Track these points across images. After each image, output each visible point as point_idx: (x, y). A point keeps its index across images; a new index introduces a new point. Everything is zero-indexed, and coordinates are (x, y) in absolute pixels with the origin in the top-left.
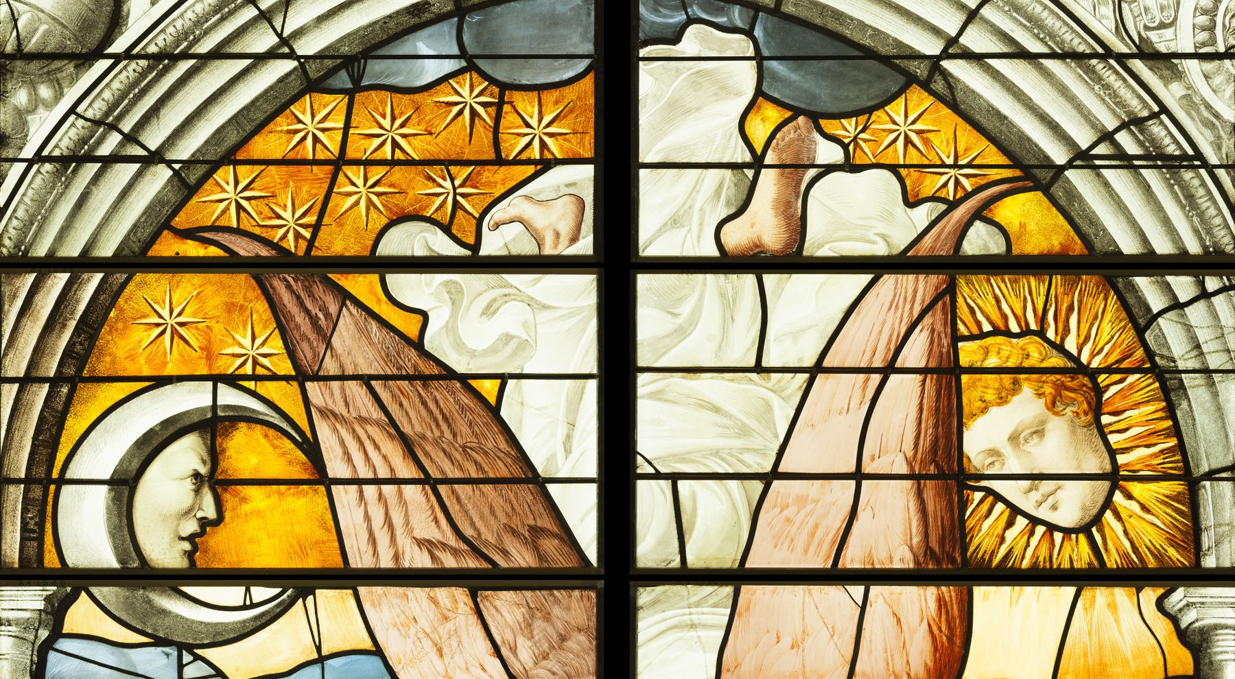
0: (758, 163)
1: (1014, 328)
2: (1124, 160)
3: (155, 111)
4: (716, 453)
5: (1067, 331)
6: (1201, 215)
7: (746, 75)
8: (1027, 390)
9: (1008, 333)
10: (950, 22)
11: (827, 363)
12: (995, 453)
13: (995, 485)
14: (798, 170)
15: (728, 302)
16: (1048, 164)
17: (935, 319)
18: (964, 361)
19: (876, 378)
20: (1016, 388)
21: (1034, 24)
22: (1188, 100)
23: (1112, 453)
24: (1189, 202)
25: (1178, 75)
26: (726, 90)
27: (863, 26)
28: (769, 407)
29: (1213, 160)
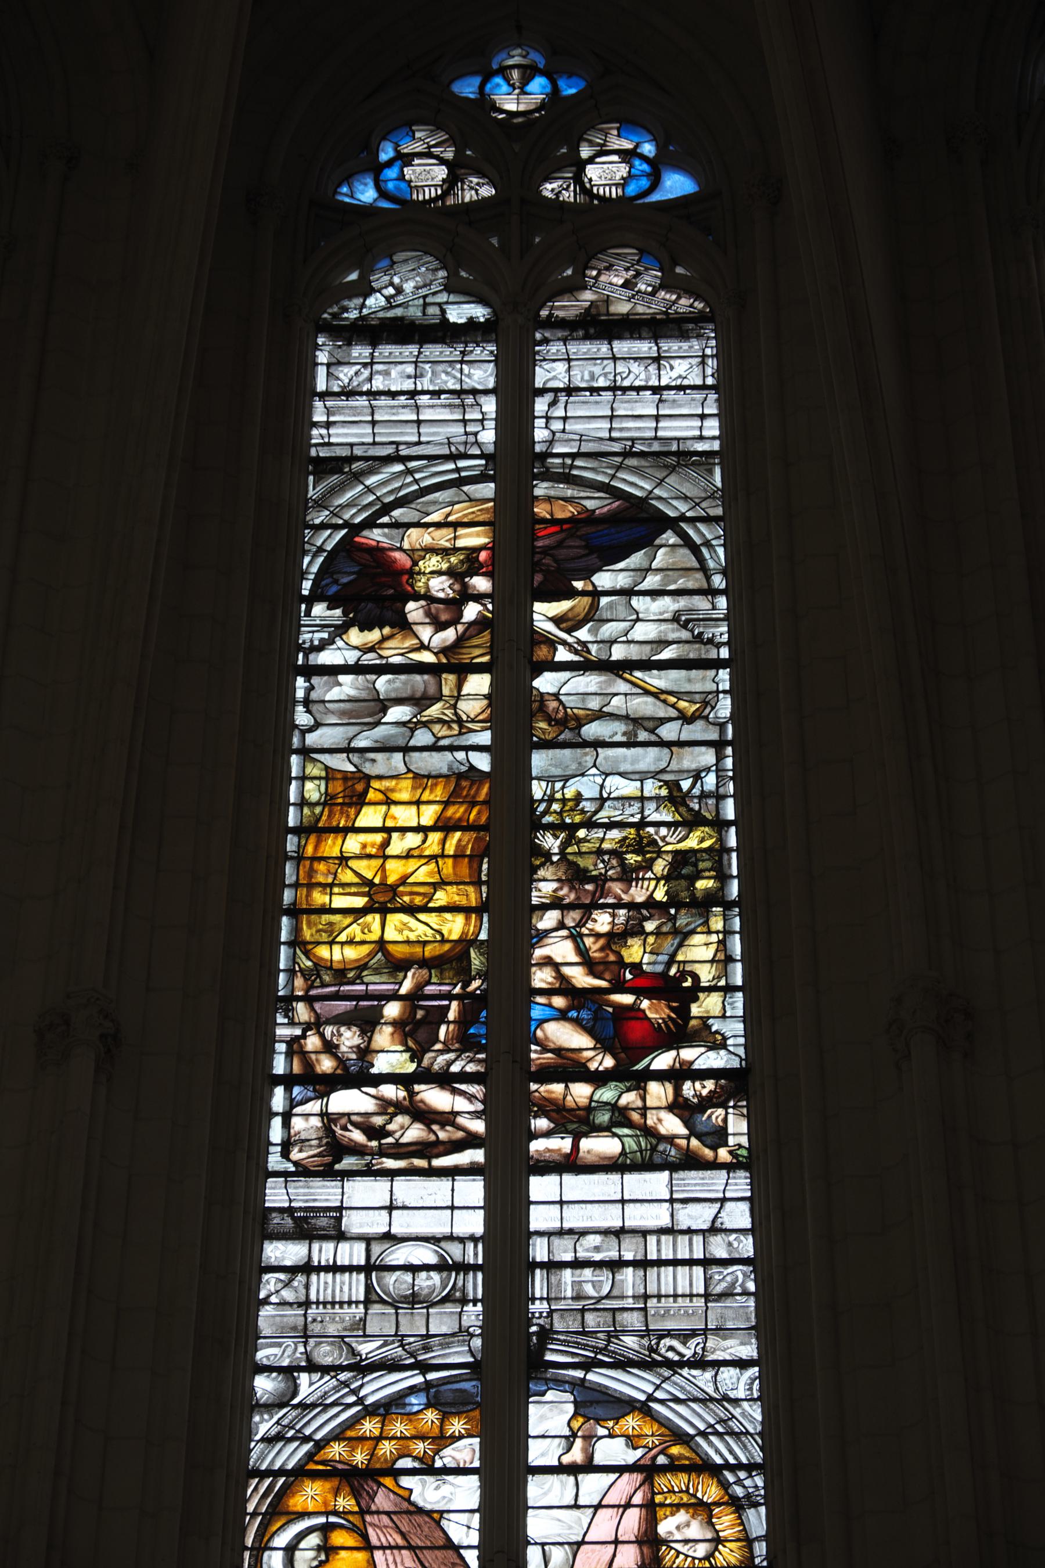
0: (574, 1435)
1: (676, 1489)
2: (717, 1433)
3: (308, 1423)
4: (559, 1535)
5: (697, 1490)
6: (749, 1452)
7: (570, 1408)
8: (682, 1511)
9: (674, 1492)
10: (650, 1389)
11: (604, 1503)
12: (670, 1533)
13: (672, 1545)
14: (590, 1439)
15: (563, 1485)
16: (688, 1434)
17: (646, 1487)
18: (657, 1501)
19: (621, 1510)
20: (678, 1511)
21: (682, 1389)
22: (743, 1414)
23: (717, 1532)
24: (744, 1447)
25: (740, 1406)
26: (562, 1412)
27: (615, 1390)
28: (580, 1519)
29: (752, 1431)
